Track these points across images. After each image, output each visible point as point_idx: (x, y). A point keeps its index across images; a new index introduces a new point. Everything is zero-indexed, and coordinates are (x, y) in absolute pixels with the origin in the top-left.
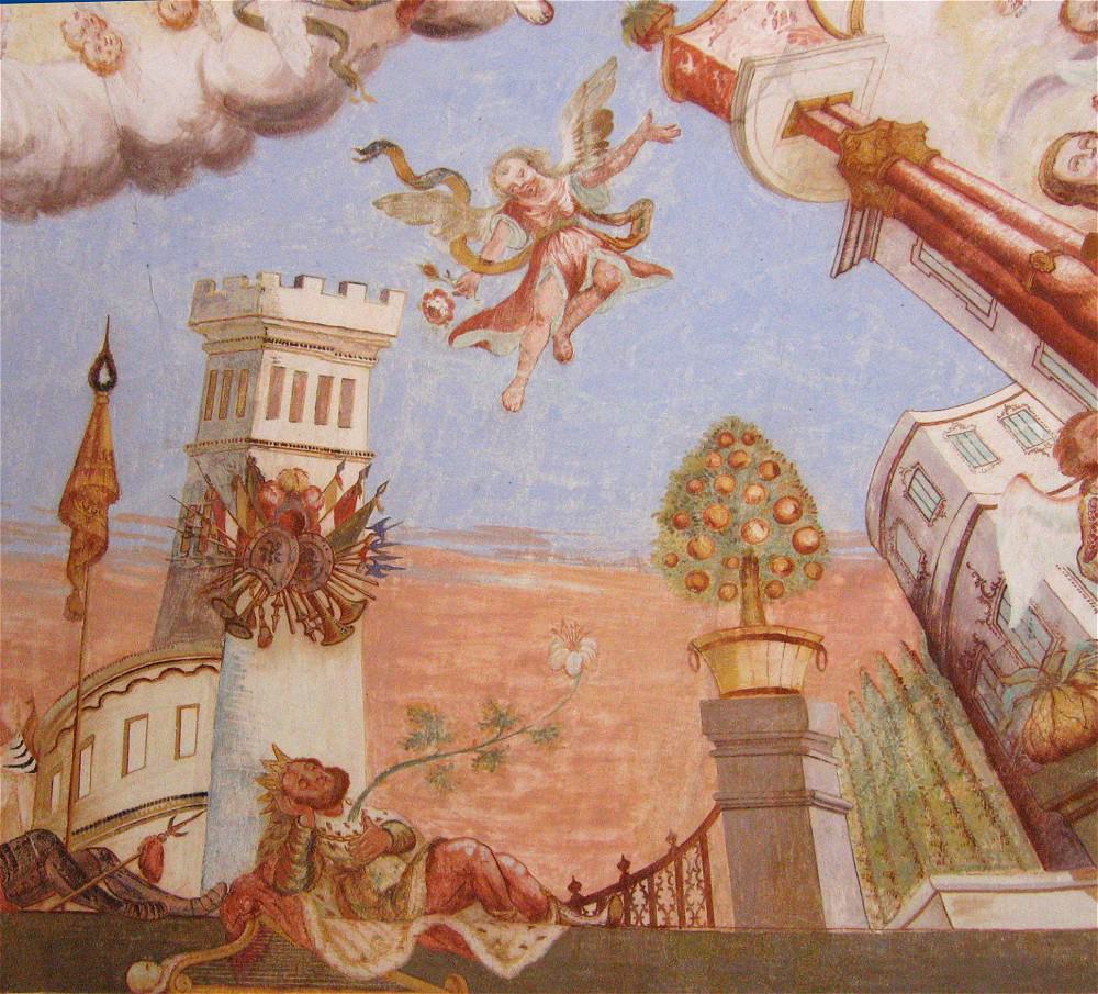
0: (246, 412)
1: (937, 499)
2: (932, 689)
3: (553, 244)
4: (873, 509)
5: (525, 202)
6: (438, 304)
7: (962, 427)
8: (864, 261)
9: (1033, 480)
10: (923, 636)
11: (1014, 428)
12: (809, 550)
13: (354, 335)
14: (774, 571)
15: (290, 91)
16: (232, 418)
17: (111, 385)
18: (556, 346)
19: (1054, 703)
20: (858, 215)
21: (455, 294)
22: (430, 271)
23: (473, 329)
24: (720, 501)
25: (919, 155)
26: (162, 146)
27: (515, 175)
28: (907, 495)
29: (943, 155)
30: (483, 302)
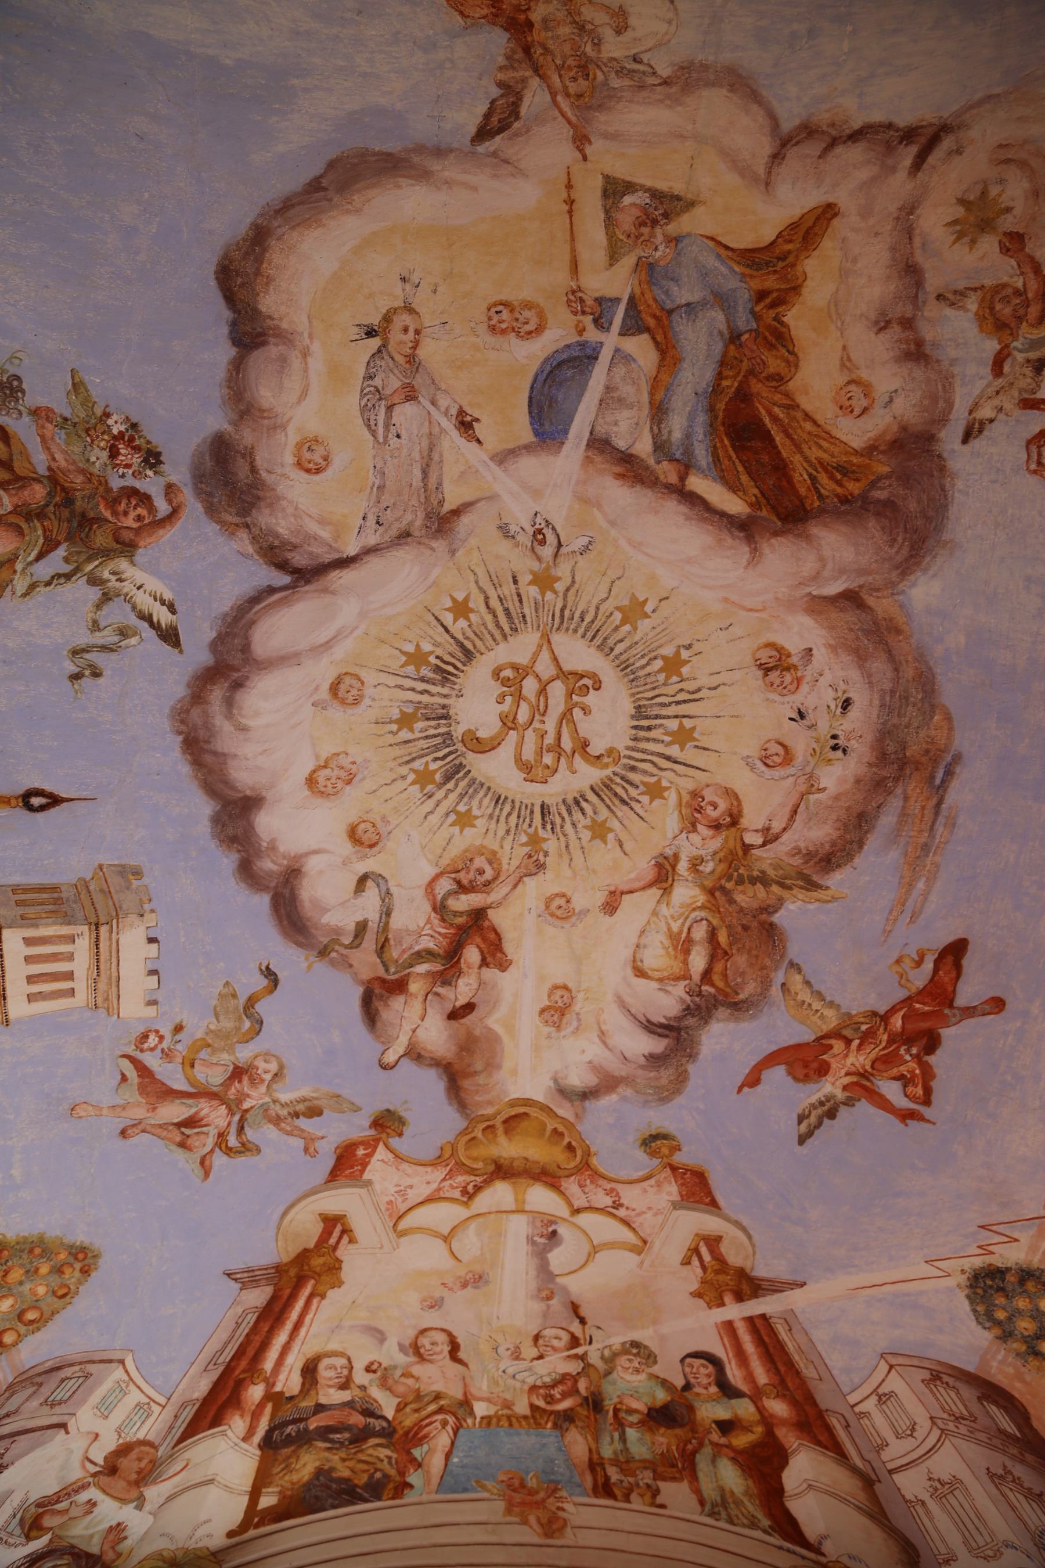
0: (24, 921)
1: (65, 1398)
3: (215, 1103)
5: (245, 1079)
6: (153, 1040)
7: (127, 1386)
8: (240, 1285)
9: (96, 1444)
13: (114, 989)
15: (309, 914)
16: (20, 911)
17: (31, 808)
18: (134, 1126)
20: (273, 1271)
21: (163, 1050)
22: (178, 1029)
23: (136, 1068)
24: (27, 1272)
25: (321, 1288)
26: (254, 829)
27: (266, 1068)
28: (63, 1381)
29: (324, 1302)
30: (160, 1069)
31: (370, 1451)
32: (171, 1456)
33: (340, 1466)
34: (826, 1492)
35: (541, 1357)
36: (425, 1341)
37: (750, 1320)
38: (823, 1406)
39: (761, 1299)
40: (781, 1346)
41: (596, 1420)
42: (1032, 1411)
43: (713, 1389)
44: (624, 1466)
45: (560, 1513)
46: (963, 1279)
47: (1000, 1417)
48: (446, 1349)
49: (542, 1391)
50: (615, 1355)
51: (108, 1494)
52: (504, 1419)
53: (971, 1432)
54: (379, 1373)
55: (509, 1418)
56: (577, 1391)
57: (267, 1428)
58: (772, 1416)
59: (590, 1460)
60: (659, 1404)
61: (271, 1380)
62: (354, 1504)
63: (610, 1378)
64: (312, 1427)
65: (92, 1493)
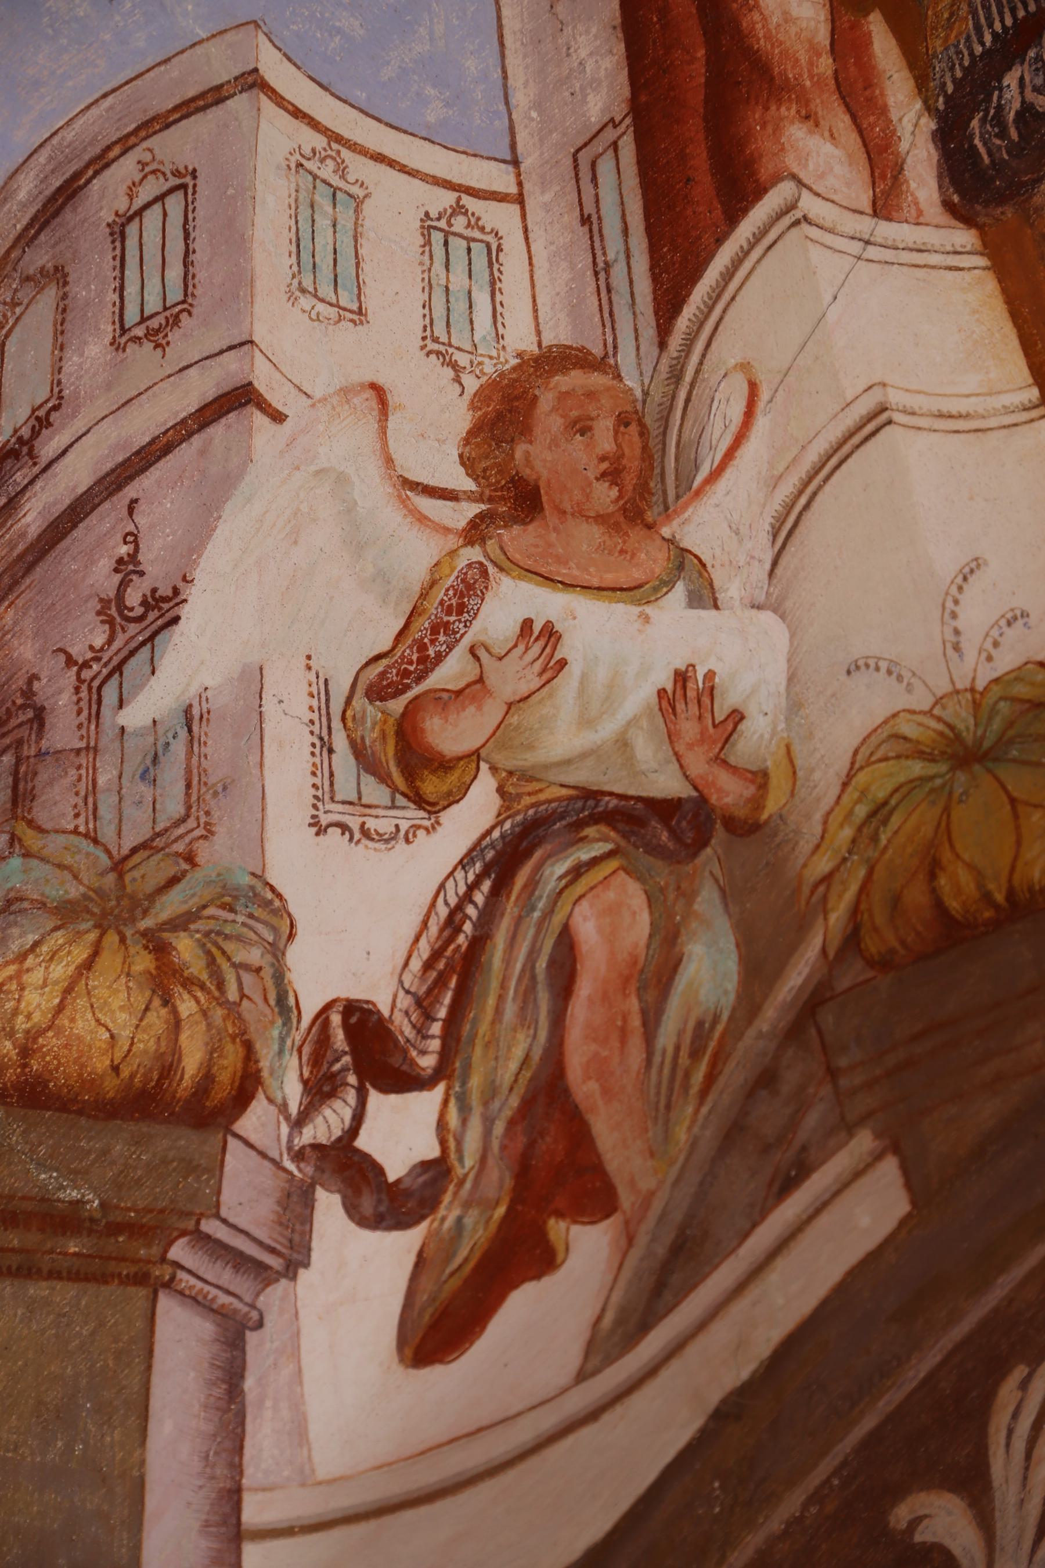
1: (175, 295)
4: (22, 195)
7: (341, 170)
11: (438, 267)
19: (88, 965)
28: (118, 232)
32: (676, 375)
51: (567, 586)
57: (929, 124)
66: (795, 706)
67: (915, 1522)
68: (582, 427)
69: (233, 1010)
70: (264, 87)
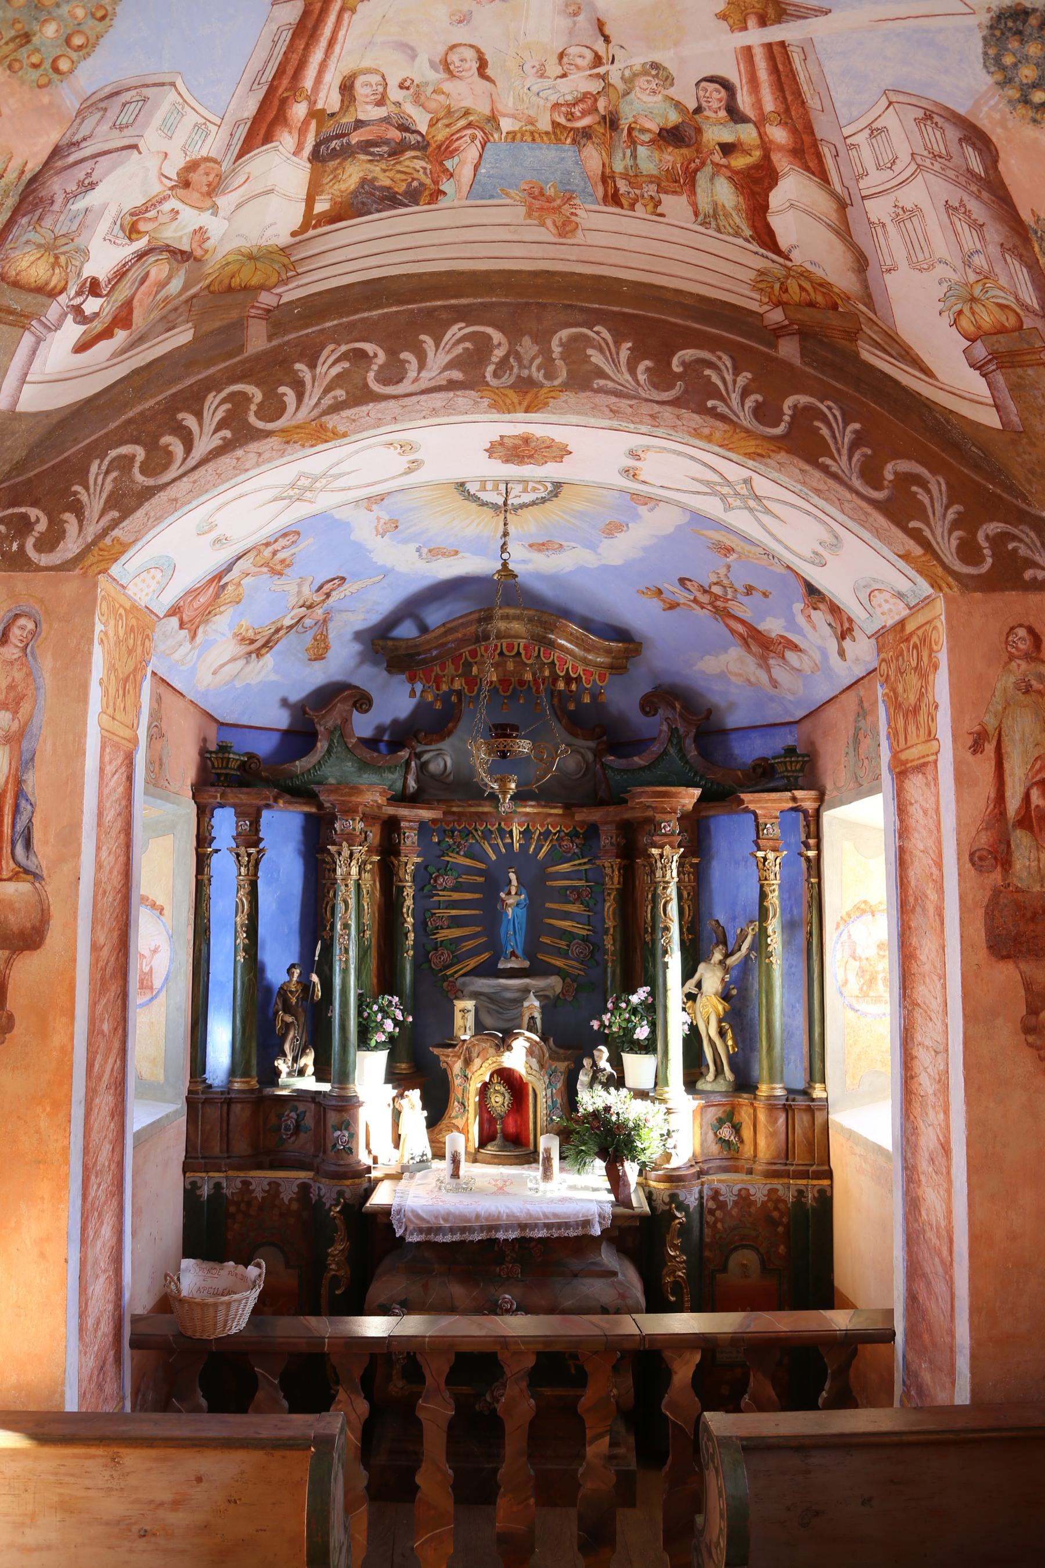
1: (131, 121)
2: (8, 197)
7: (183, 108)
10: (37, 169)
12: (56, 70)
14: (28, 57)
28: (124, 105)
29: (354, 17)
31: (407, 163)
32: (234, 170)
33: (381, 176)
34: (805, 211)
35: (564, 76)
36: (454, 58)
37: (769, 47)
38: (819, 135)
39: (784, 25)
40: (793, 75)
41: (611, 137)
42: (1002, 155)
43: (723, 113)
44: (633, 180)
45: (573, 218)
46: (985, 18)
47: (973, 159)
48: (475, 65)
49: (563, 109)
50: (635, 75)
52: (528, 134)
53: (943, 169)
54: (412, 90)
55: (532, 133)
56: (597, 110)
58: (771, 142)
59: (603, 173)
60: (670, 125)
61: (313, 98)
62: (396, 208)
63: (628, 98)
64: (353, 142)
65: (173, 204)
66: (222, 239)
67: (183, 419)
68: (207, 174)
69: (67, 274)
70: (175, 86)
